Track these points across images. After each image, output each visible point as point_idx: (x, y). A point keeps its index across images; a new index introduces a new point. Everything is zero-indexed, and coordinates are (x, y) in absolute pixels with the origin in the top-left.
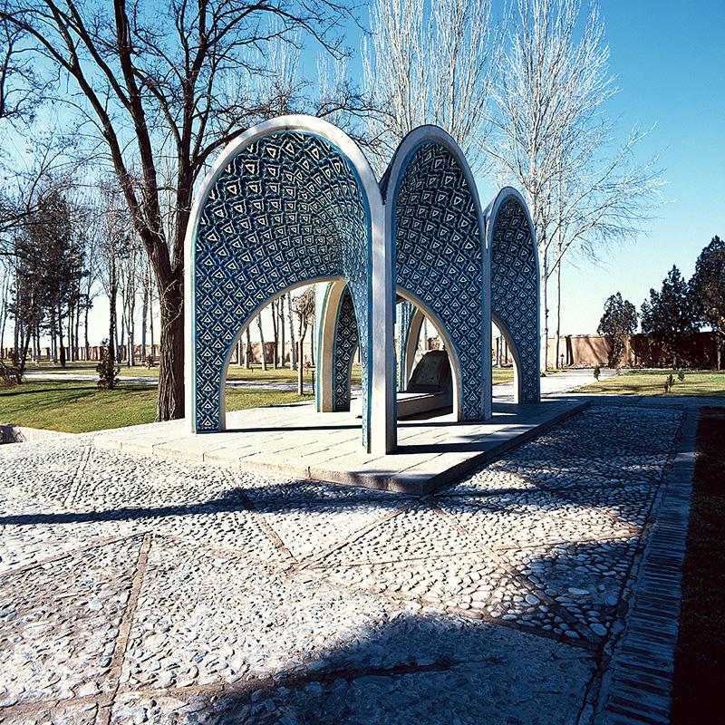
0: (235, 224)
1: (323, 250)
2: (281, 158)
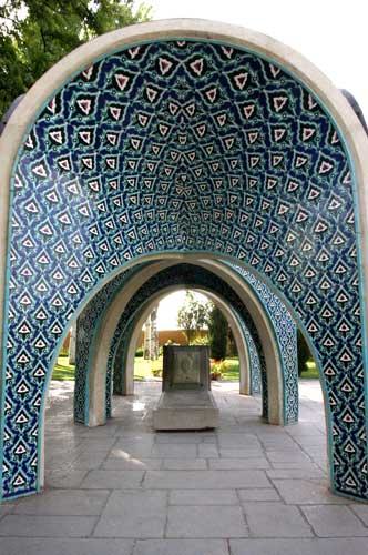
2: (174, 78)
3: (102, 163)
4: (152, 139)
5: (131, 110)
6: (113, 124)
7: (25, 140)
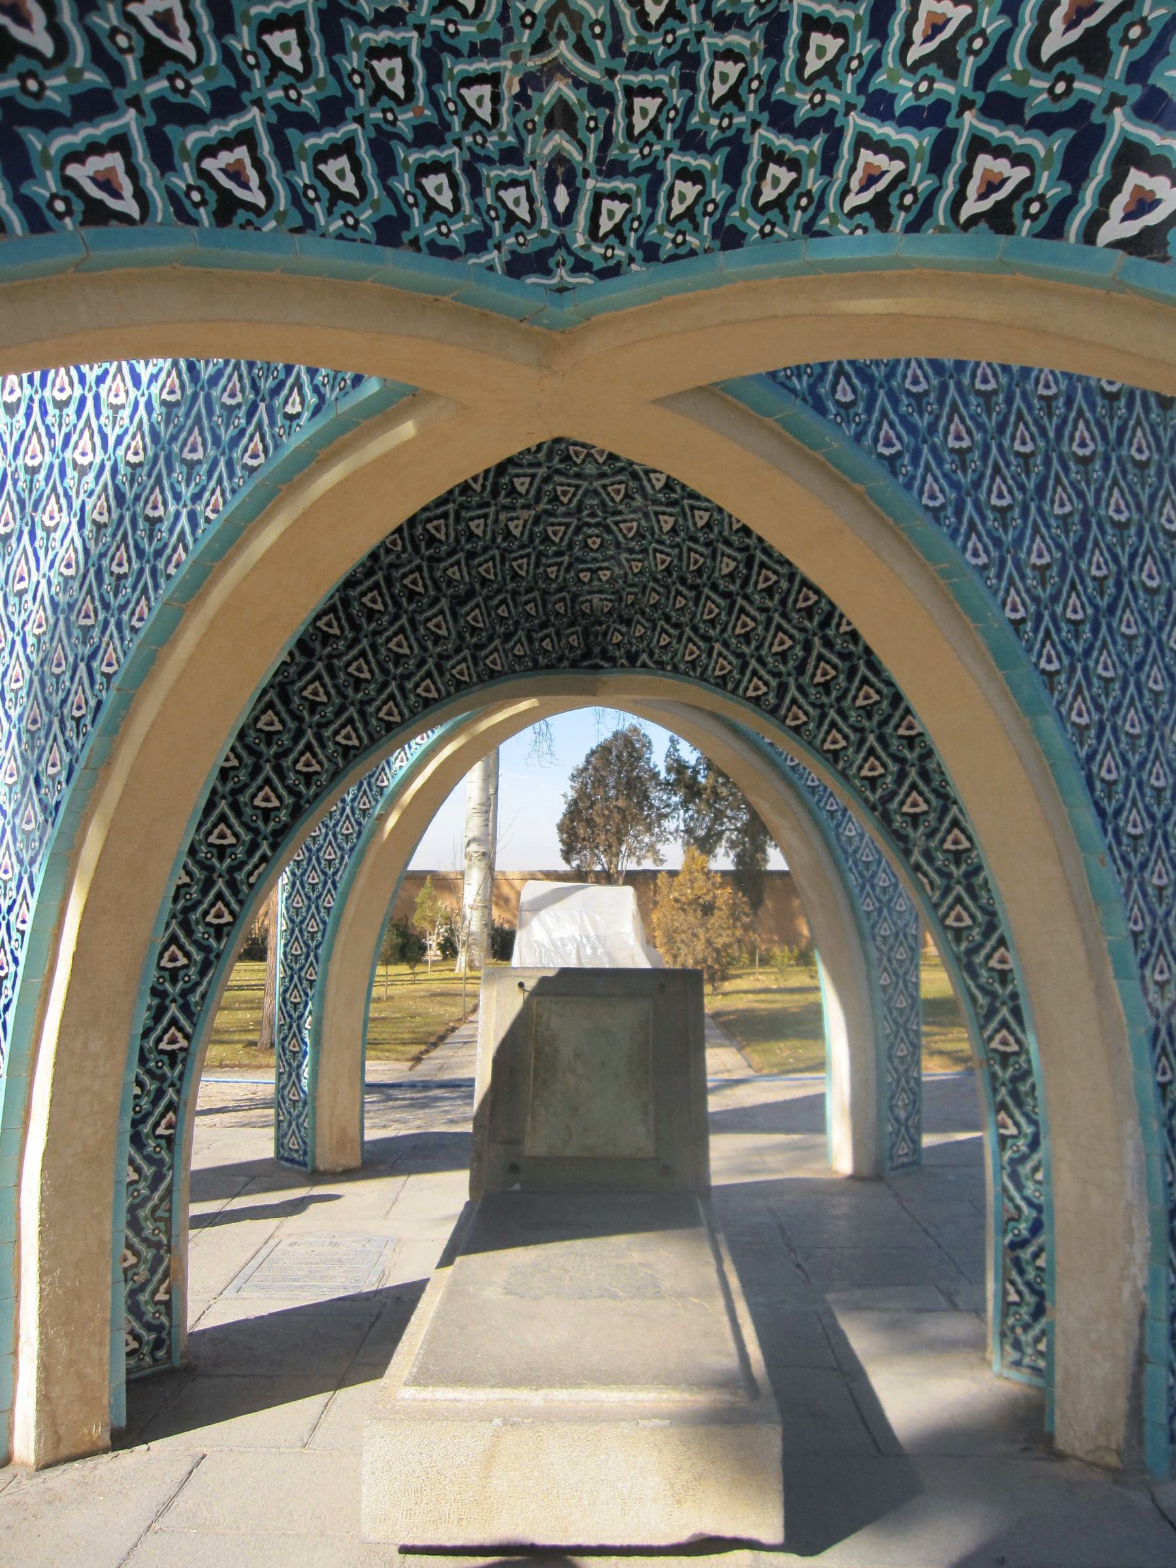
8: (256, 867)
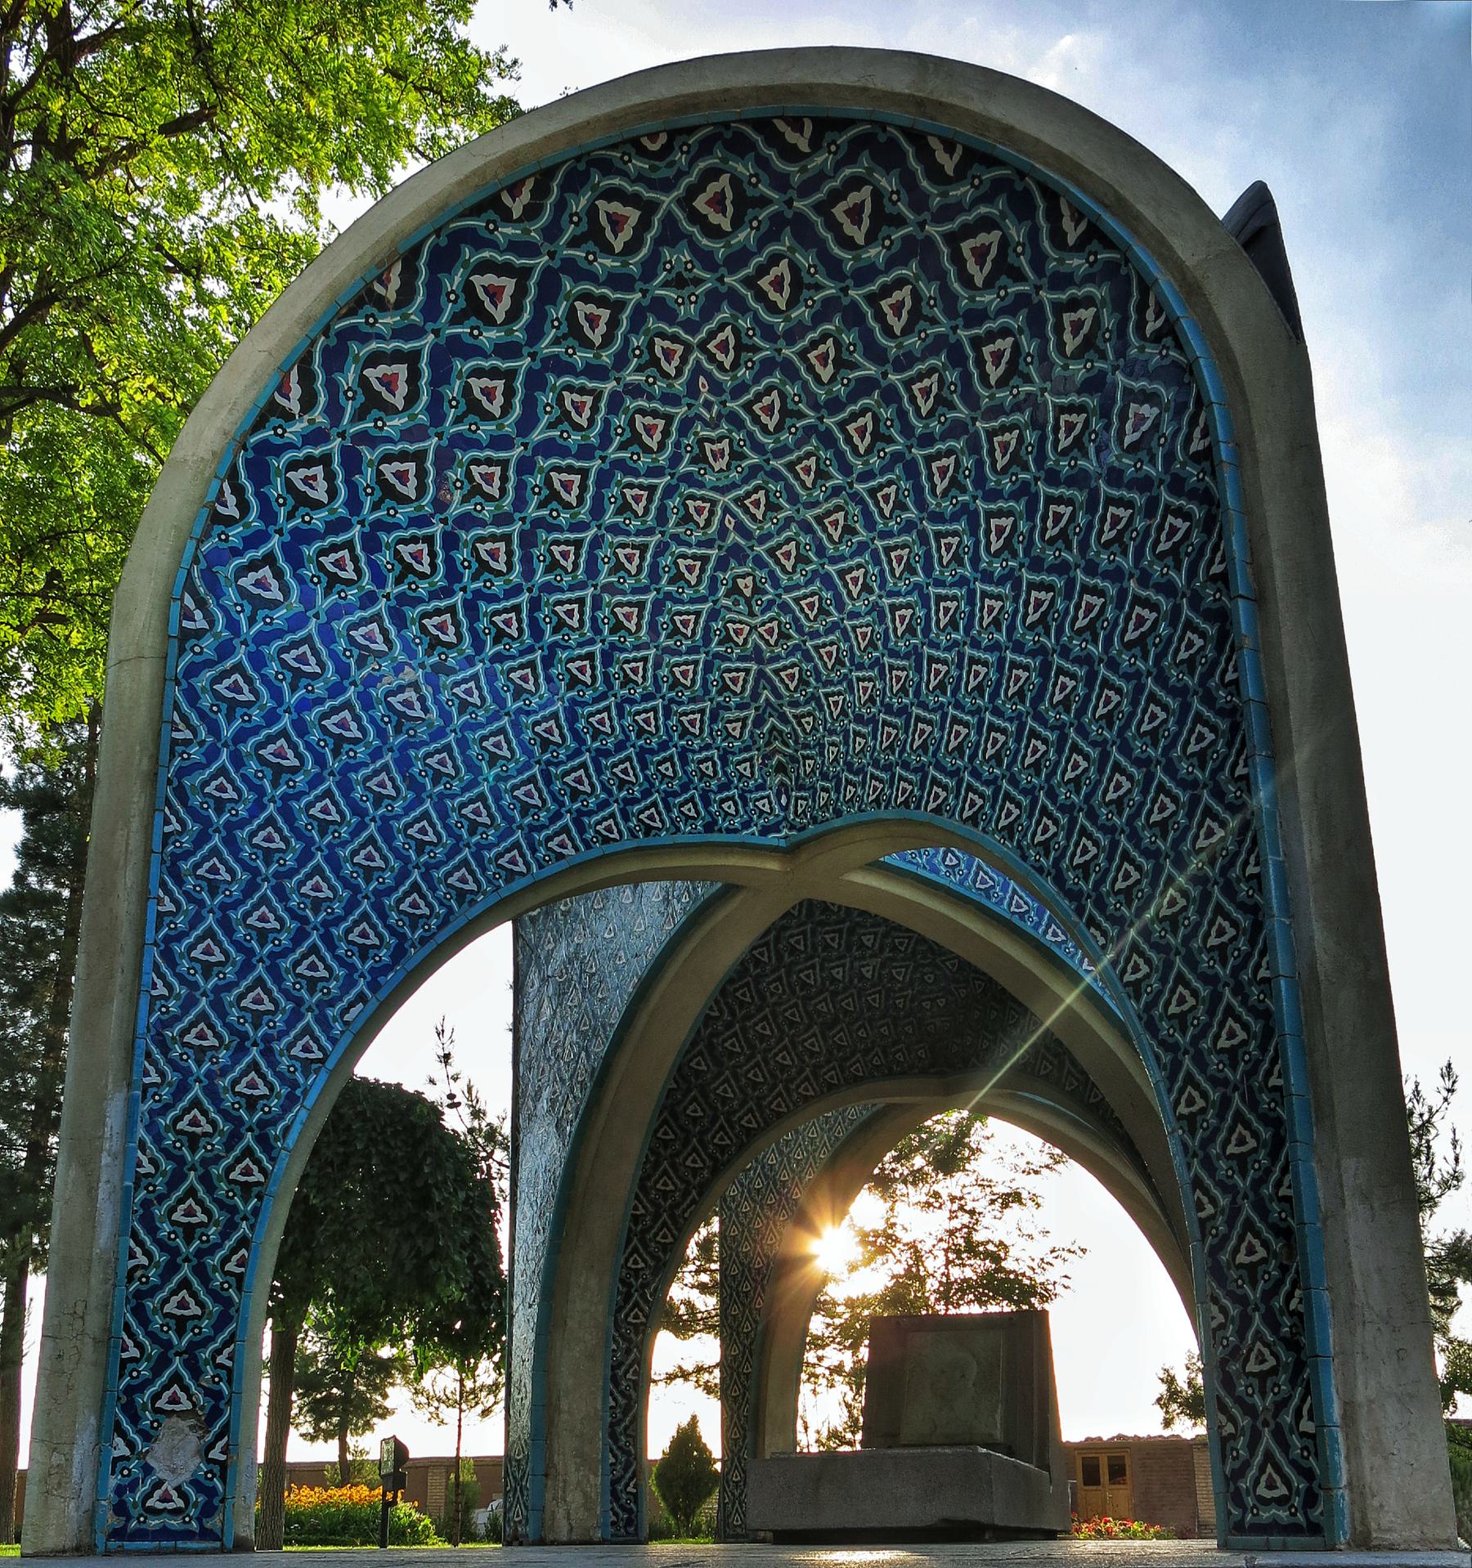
0: (371, 544)
1: (735, 729)
3: (462, 555)
4: (619, 464)
5: (536, 382)
6: (486, 430)
7: (212, 496)
8: (352, 1005)
